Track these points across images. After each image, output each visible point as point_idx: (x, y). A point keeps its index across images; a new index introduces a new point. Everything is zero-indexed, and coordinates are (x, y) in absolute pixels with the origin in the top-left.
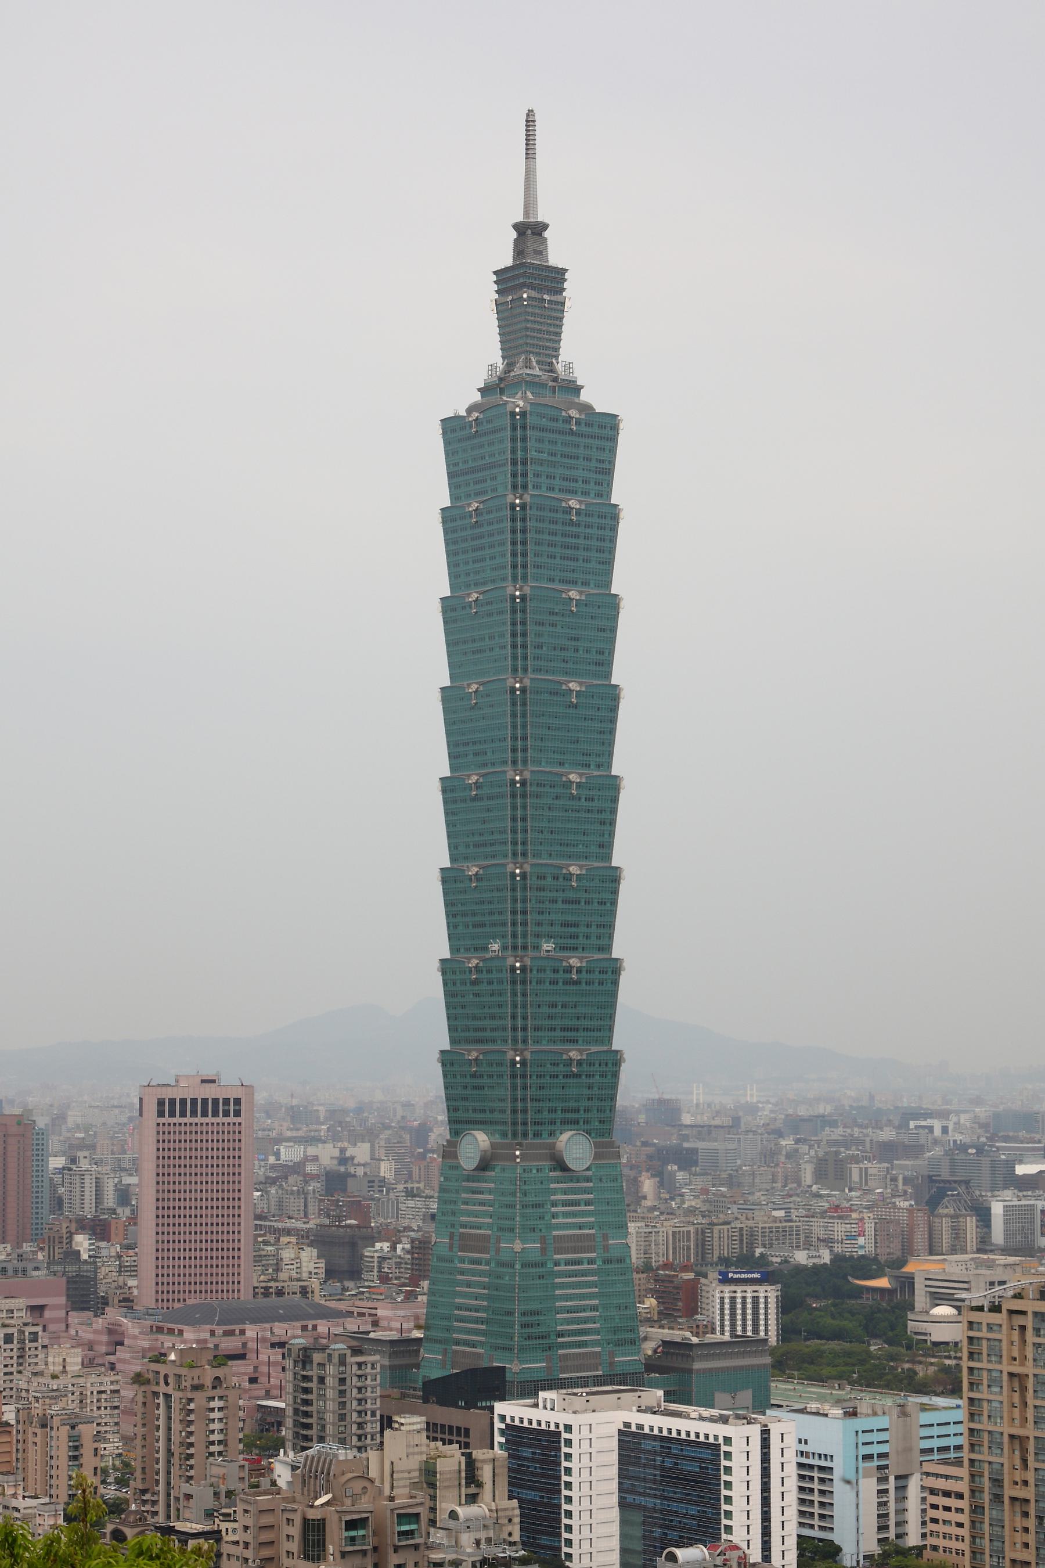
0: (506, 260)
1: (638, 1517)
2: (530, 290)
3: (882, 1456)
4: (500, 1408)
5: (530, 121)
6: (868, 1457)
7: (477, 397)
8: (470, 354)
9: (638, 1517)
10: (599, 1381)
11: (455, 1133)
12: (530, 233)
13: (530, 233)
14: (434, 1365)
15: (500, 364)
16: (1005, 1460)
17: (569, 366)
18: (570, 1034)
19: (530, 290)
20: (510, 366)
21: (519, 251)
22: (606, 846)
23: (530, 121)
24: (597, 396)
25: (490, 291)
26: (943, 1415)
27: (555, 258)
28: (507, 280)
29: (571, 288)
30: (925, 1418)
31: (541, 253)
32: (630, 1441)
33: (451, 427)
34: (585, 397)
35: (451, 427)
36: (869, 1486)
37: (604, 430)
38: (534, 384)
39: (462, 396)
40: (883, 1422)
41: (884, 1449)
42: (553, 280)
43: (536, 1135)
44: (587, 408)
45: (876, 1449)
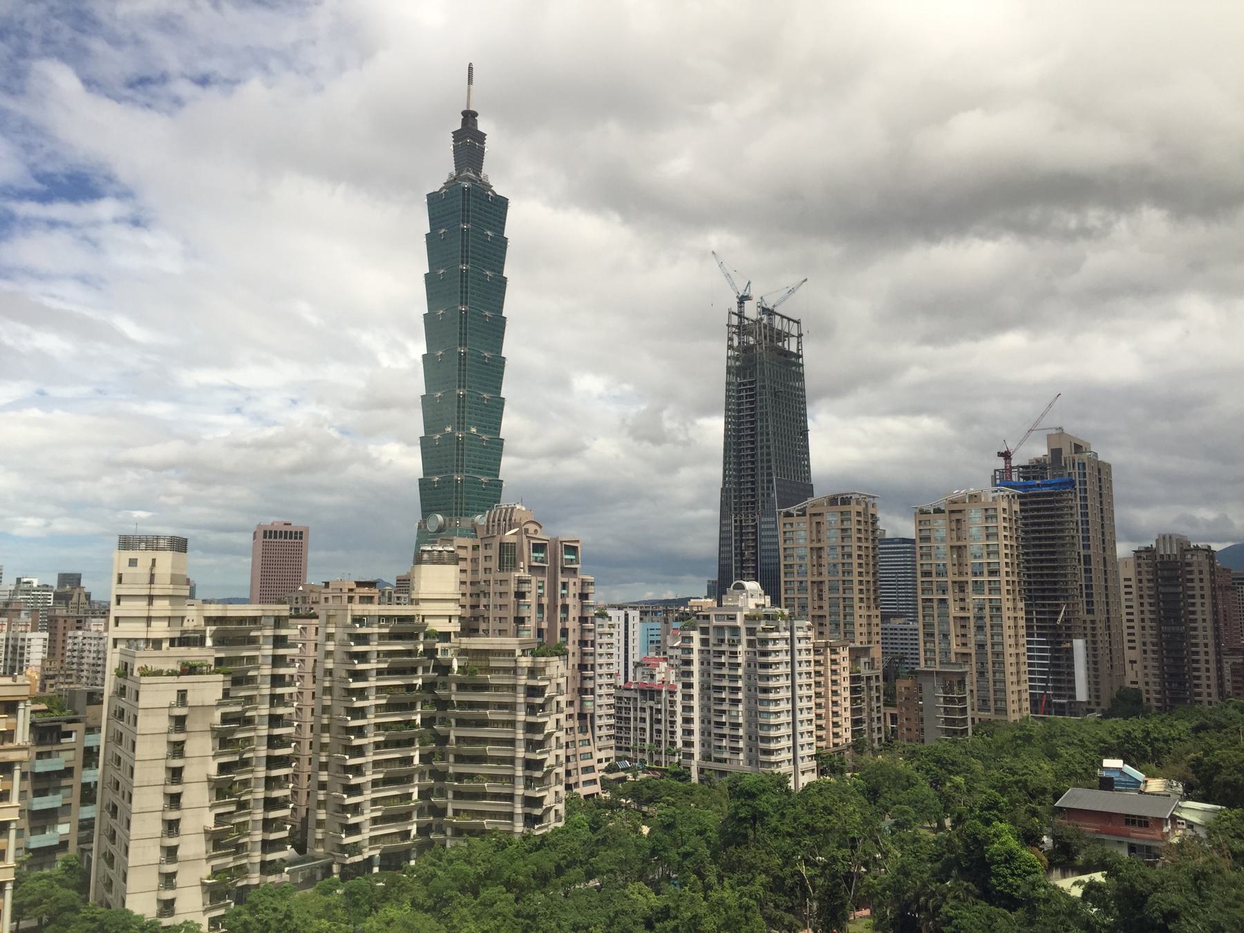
0: (458, 126)
2: (469, 143)
3: (658, 642)
5: (470, 69)
6: (652, 642)
8: (440, 168)
12: (469, 117)
13: (469, 117)
16: (809, 596)
19: (469, 143)
20: (458, 174)
21: (464, 122)
23: (470, 69)
24: (499, 189)
28: (457, 135)
33: (433, 199)
35: (433, 199)
37: (501, 205)
38: (470, 180)
39: (437, 185)
41: (659, 638)
43: (467, 515)
45: (655, 638)
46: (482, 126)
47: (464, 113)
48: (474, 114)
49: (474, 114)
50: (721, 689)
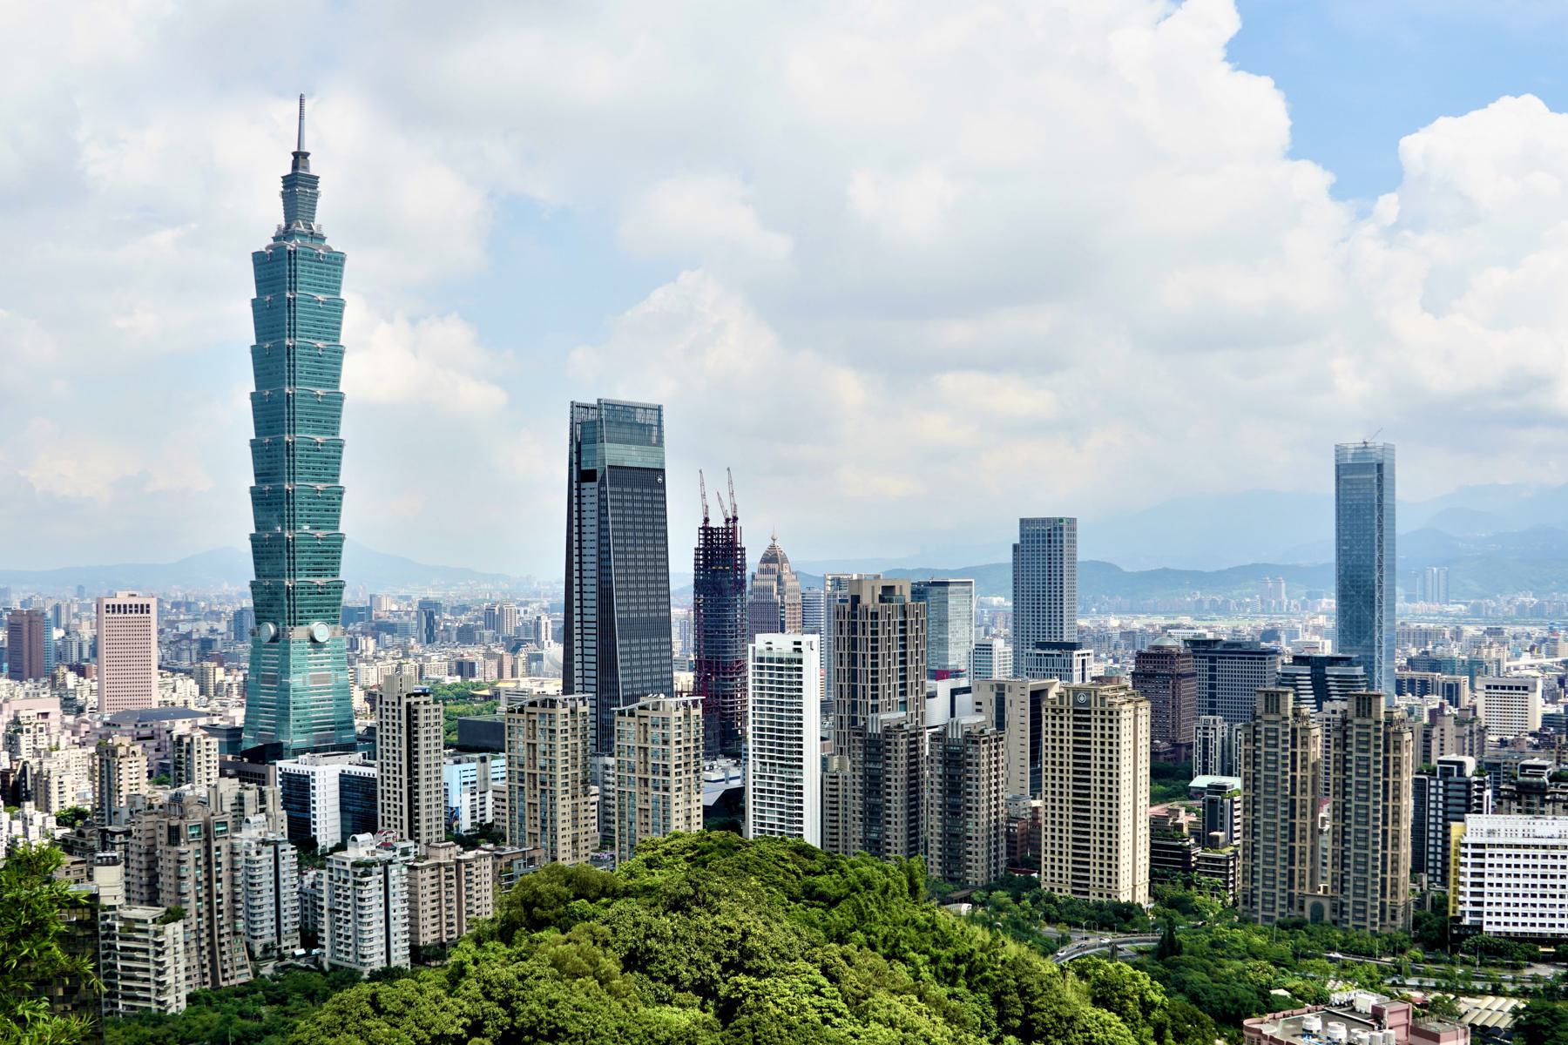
0: (288, 171)
1: (349, 816)
2: (298, 187)
4: (279, 763)
7: (271, 242)
9: (349, 816)
10: (333, 749)
11: (258, 623)
12: (300, 157)
13: (300, 157)
14: (249, 741)
15: (283, 224)
17: (319, 227)
18: (318, 570)
19: (298, 187)
20: (288, 226)
21: (295, 166)
22: (335, 476)
24: (334, 243)
25: (280, 187)
26: (498, 765)
27: (313, 171)
28: (286, 179)
29: (321, 187)
30: (494, 763)
31: (306, 168)
32: (346, 781)
33: (258, 257)
34: (327, 242)
35: (258, 257)
36: (467, 797)
39: (264, 242)
40: (473, 766)
42: (313, 181)
44: (329, 249)
46: (314, 167)
47: (296, 155)
48: (306, 155)
49: (306, 155)
50: (339, 912)
